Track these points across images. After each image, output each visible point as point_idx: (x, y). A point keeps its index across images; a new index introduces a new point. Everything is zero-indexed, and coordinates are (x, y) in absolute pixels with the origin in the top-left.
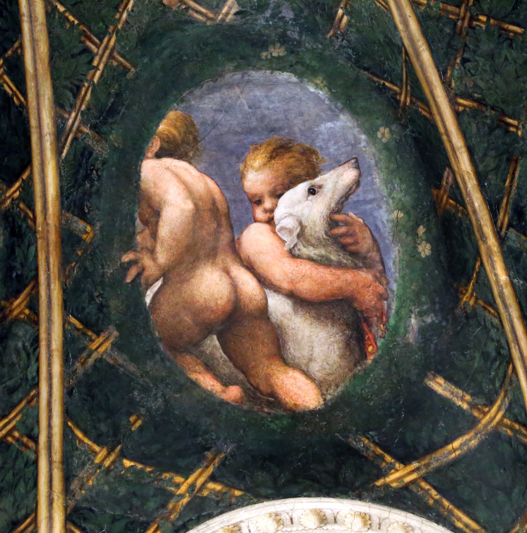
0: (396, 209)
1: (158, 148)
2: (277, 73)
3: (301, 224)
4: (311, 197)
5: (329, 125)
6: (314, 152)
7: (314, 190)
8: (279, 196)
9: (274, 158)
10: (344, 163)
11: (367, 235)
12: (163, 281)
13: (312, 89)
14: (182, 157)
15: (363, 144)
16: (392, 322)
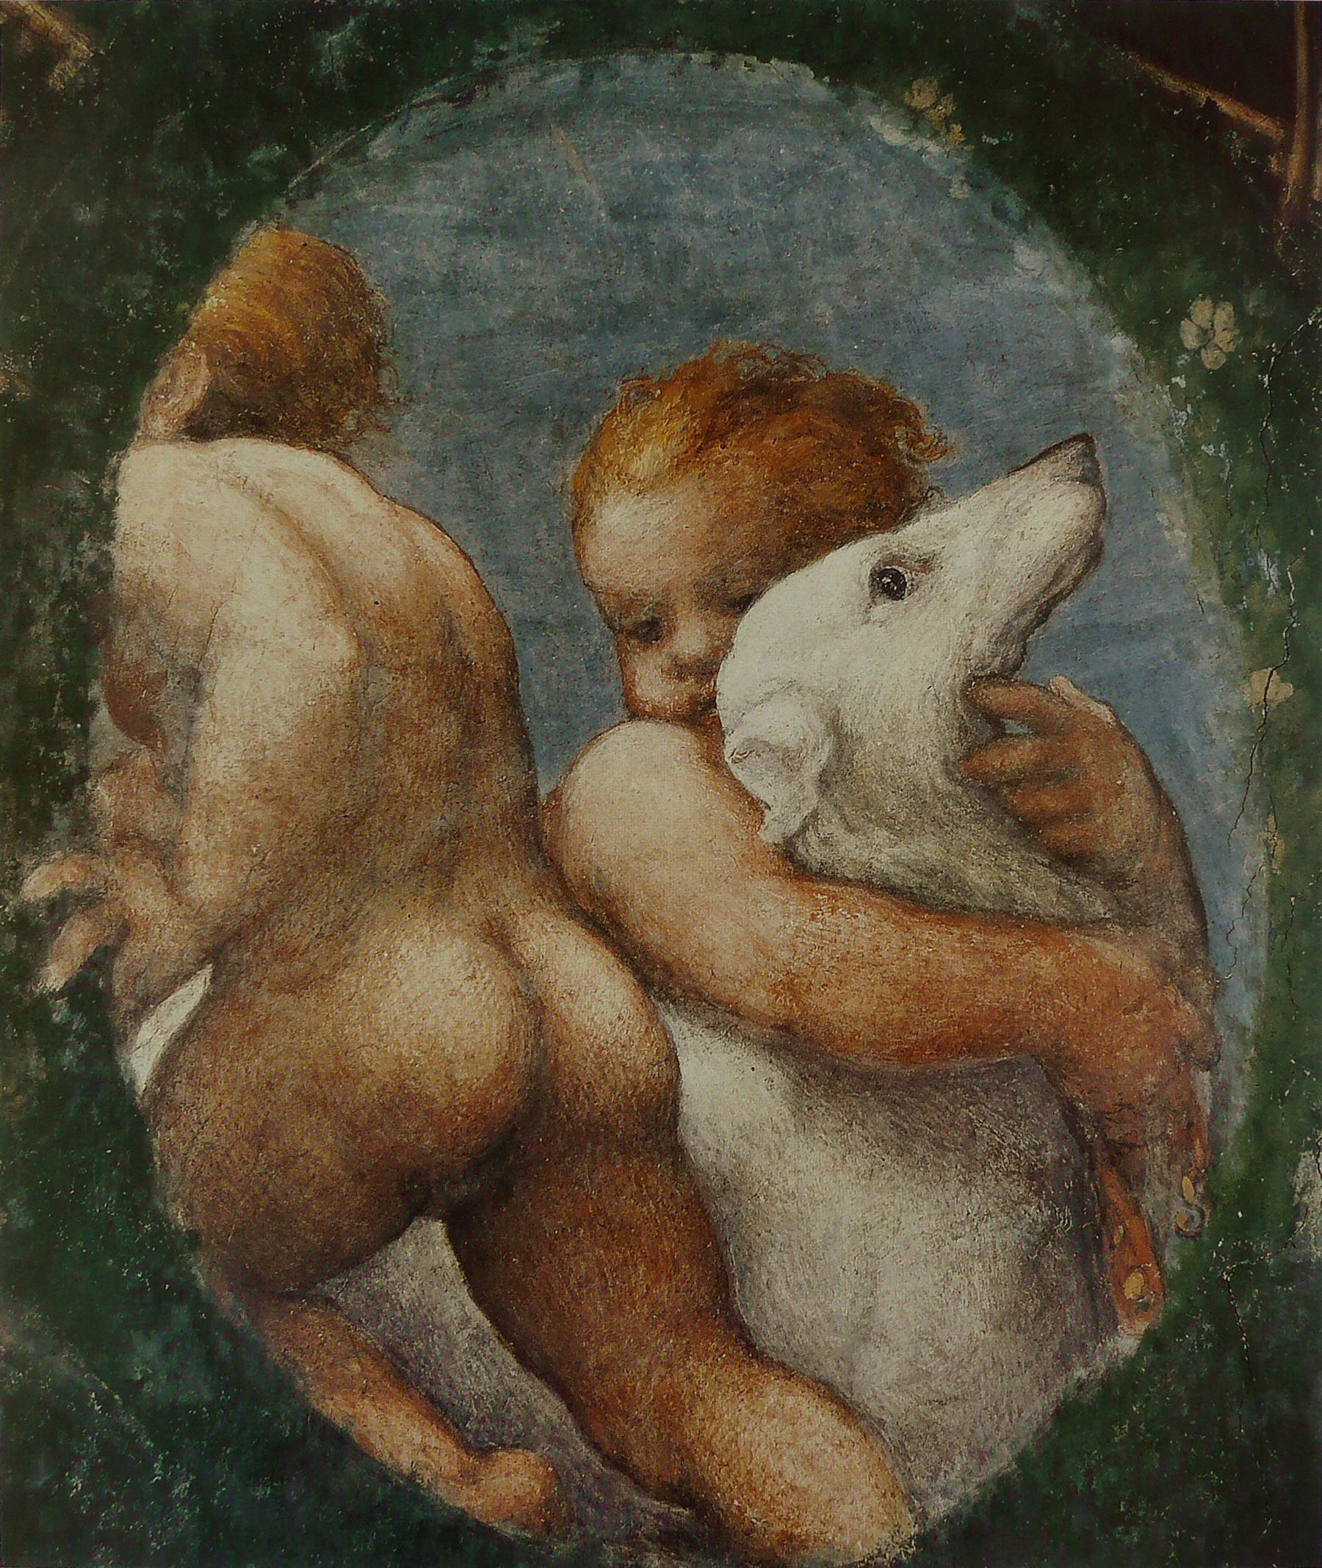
0: (1262, 666)
1: (198, 393)
2: (737, 64)
3: (835, 727)
4: (884, 608)
5: (966, 292)
6: (900, 413)
7: (897, 577)
8: (743, 603)
9: (722, 437)
10: (1033, 461)
11: (1132, 777)
12: (213, 979)
13: (894, 136)
14: (295, 434)
15: (1118, 375)
16: (1233, 1165)
